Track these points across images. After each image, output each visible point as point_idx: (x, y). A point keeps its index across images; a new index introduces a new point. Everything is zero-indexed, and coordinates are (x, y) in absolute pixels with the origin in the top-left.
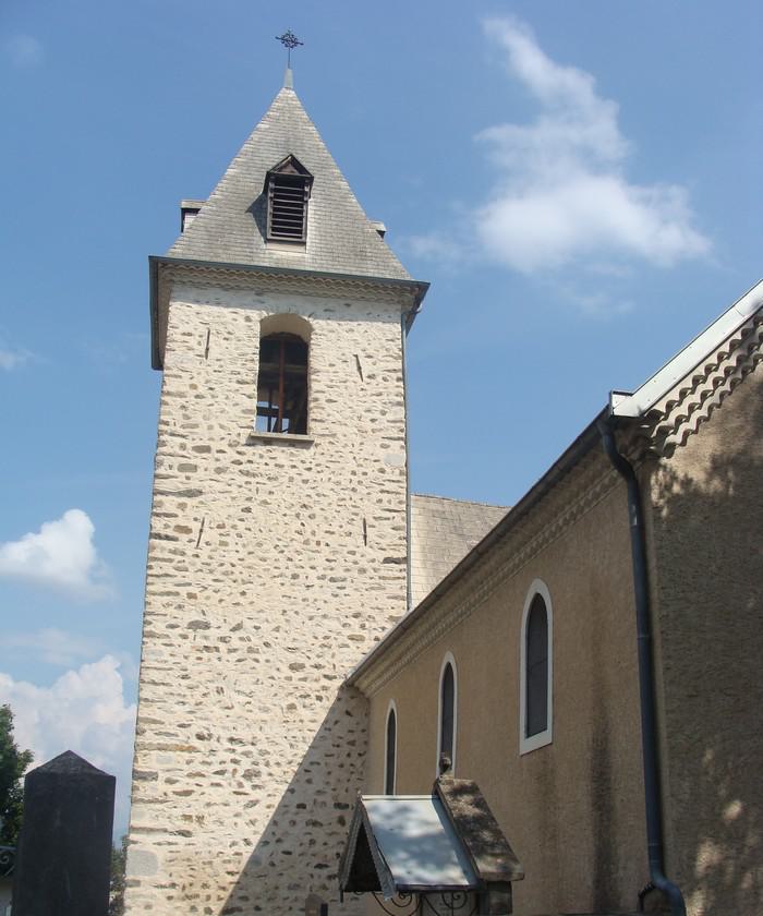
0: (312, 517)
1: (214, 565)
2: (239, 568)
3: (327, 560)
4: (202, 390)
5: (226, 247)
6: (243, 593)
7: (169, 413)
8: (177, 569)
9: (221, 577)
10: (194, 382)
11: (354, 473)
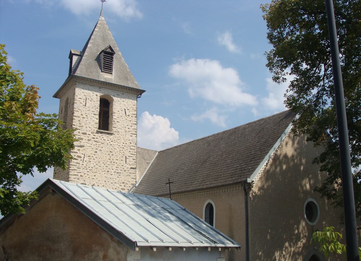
0: (113, 155)
1: (87, 167)
2: (94, 168)
3: (116, 167)
4: (84, 116)
5: (91, 73)
6: (95, 176)
7: (76, 122)
8: (78, 168)
9: (89, 171)
10: (82, 113)
11: (123, 143)
